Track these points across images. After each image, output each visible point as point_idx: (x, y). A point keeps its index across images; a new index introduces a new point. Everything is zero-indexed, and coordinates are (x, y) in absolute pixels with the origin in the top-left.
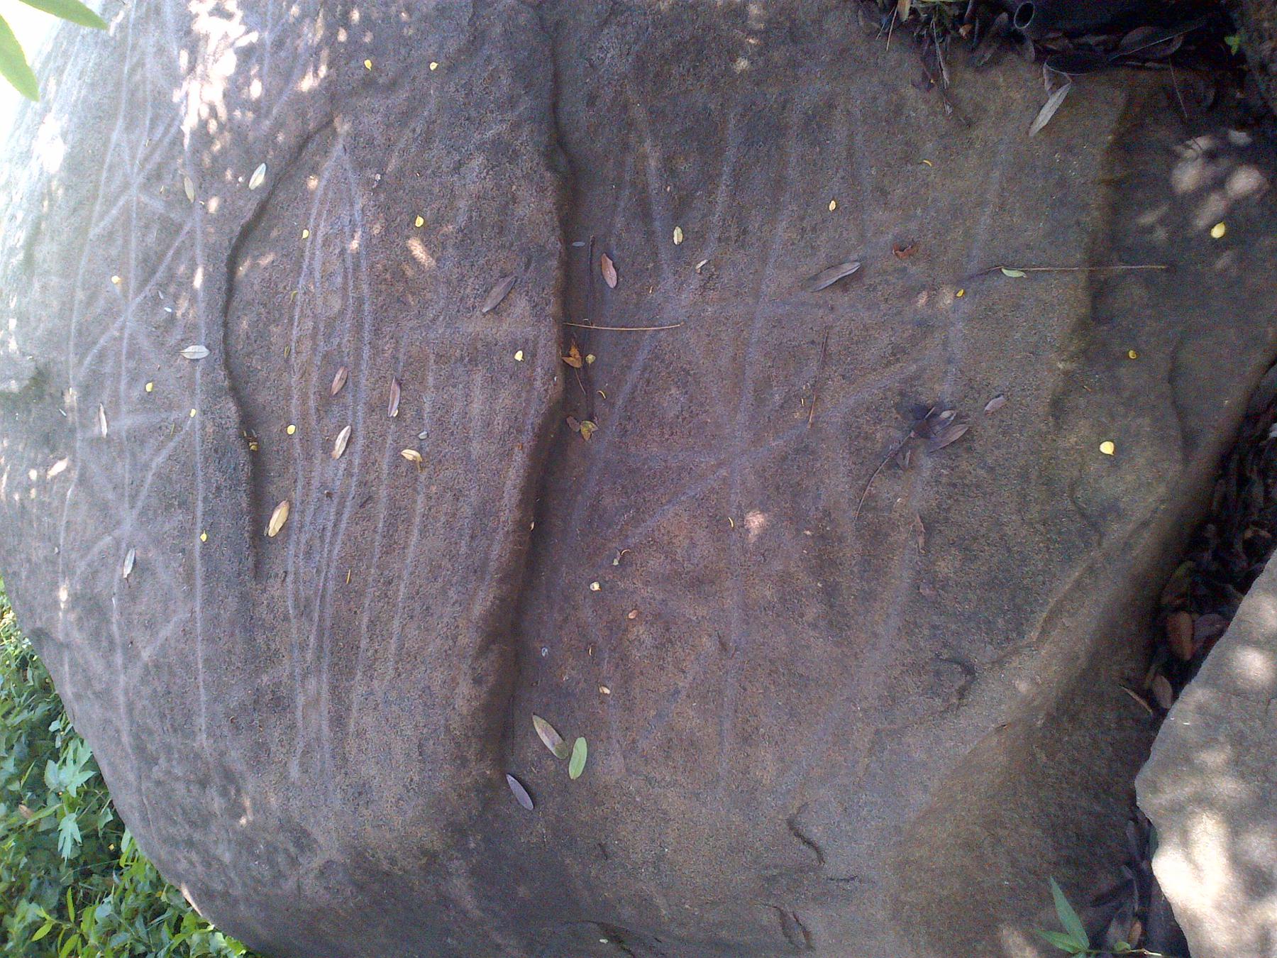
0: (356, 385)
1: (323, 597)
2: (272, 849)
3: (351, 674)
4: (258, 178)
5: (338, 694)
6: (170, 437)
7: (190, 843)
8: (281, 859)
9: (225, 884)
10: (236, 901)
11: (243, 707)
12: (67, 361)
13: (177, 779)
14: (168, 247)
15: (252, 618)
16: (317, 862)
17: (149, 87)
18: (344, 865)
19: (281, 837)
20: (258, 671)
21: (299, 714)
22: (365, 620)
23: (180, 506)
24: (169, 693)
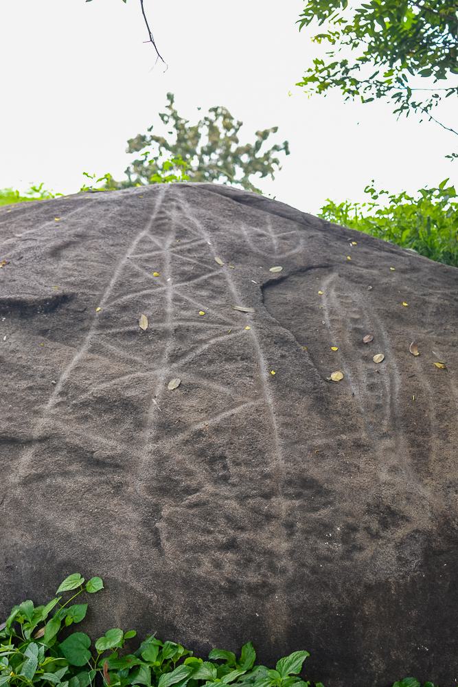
0: (382, 343)
1: (392, 405)
2: (354, 529)
3: (425, 433)
4: (276, 270)
5: (413, 443)
6: (227, 333)
7: (231, 545)
8: (360, 536)
9: (264, 576)
10: (272, 591)
11: (328, 447)
12: (101, 296)
13: (227, 498)
14: (203, 275)
15: (327, 409)
16: (401, 533)
17: (173, 227)
18: (428, 535)
19: (367, 517)
20: (337, 433)
21: (379, 454)
22: (433, 415)
23: (242, 359)
24: (232, 444)
